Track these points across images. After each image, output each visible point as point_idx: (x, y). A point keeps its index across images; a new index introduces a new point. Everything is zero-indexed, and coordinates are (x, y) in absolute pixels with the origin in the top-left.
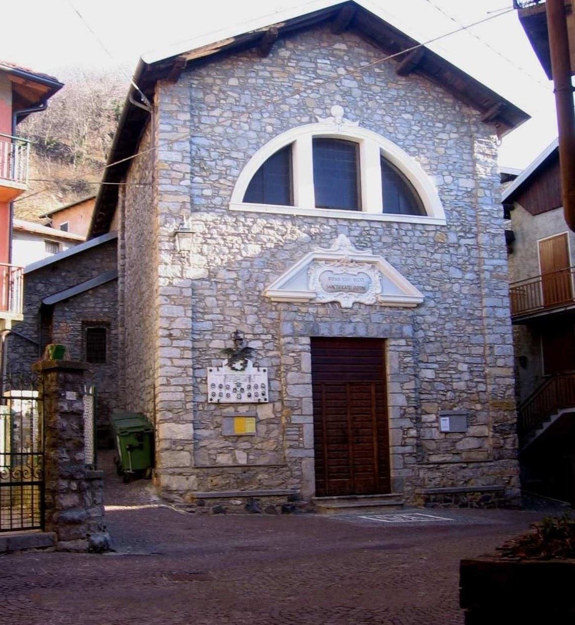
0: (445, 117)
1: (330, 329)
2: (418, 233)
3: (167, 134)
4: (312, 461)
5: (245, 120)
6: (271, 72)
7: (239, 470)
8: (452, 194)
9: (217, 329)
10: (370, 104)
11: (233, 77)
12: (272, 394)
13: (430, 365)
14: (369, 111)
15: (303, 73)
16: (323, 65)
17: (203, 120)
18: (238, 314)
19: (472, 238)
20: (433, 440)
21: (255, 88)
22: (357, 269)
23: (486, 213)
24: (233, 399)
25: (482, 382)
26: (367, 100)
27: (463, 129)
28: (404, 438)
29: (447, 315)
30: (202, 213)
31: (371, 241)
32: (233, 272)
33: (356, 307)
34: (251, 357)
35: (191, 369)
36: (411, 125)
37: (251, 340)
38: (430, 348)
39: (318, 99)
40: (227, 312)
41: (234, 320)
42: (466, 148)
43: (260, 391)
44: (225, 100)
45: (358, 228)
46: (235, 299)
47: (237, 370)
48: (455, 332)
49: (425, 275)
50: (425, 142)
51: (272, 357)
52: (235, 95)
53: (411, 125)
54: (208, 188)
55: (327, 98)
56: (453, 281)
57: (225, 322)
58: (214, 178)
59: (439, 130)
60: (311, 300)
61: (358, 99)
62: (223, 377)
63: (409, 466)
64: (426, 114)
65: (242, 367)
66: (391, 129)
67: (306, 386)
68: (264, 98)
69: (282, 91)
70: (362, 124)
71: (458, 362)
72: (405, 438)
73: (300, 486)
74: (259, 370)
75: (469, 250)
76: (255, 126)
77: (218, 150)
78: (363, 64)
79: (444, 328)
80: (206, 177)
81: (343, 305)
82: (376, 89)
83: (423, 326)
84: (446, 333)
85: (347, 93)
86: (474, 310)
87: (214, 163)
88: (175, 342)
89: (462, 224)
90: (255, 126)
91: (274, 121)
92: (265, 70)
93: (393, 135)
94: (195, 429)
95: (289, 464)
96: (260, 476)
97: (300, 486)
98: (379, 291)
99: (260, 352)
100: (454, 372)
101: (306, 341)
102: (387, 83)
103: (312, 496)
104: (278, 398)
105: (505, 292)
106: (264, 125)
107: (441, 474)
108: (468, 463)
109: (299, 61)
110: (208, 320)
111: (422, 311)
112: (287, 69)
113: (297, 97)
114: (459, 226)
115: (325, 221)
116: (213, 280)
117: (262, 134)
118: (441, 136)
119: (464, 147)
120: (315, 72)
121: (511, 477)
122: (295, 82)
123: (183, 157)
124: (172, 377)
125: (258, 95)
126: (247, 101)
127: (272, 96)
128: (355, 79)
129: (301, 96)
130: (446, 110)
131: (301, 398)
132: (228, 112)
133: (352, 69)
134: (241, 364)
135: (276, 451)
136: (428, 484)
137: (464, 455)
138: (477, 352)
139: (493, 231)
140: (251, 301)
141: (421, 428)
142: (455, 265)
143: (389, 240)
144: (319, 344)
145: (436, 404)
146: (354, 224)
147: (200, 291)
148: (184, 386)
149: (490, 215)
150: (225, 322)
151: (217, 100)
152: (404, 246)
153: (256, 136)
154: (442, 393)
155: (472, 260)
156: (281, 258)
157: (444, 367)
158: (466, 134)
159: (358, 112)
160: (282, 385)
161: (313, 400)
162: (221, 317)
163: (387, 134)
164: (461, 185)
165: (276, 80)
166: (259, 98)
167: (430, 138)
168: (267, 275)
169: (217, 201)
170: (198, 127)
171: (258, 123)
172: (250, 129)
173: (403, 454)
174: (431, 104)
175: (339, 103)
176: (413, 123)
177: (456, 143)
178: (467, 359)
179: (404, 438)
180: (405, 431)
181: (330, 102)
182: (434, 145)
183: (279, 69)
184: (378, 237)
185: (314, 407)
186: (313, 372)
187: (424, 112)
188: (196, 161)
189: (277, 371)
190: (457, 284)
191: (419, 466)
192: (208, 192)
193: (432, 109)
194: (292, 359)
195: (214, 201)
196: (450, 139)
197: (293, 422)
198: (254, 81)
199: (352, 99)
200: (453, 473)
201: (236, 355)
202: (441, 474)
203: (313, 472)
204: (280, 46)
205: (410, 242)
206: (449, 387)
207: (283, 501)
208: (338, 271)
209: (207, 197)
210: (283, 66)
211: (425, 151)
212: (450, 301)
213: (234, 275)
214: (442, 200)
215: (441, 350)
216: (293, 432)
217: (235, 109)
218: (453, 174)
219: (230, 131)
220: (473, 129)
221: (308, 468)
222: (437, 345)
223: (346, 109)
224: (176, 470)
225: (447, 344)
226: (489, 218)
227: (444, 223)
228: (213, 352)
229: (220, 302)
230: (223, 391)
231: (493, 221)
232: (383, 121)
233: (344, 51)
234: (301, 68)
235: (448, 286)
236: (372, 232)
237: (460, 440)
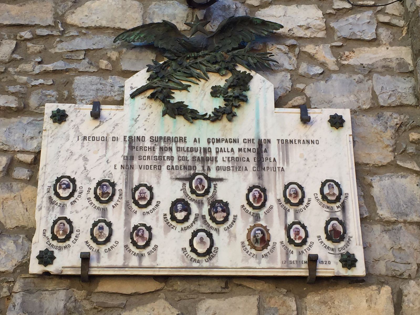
24: (170, 251)
34: (265, 66)
43: (315, 217)
47: (192, 116)
51: (369, 71)
62: (121, 149)
65: (219, 103)
74: (305, 120)
99: (310, 49)
134: (215, 92)
228: (82, 44)
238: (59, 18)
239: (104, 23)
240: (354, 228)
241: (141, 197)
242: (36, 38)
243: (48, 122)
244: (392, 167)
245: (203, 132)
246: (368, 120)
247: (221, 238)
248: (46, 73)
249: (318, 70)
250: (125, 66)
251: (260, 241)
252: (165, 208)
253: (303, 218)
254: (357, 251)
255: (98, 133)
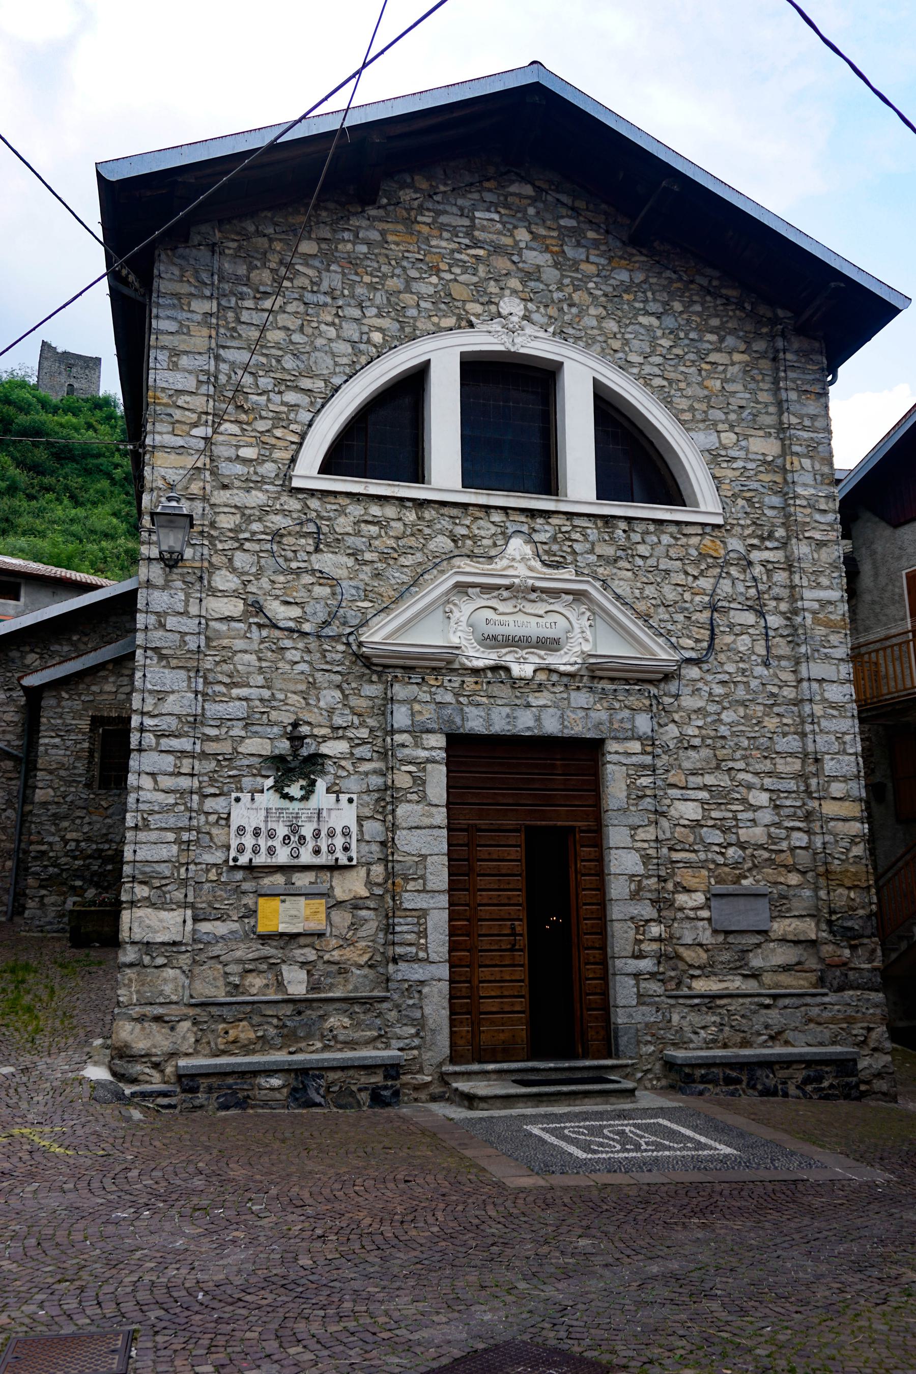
0: (722, 323)
1: (488, 720)
2: (666, 539)
3: (170, 337)
4: (445, 986)
5: (329, 319)
6: (383, 233)
7: (288, 1010)
8: (735, 466)
9: (258, 716)
10: (576, 297)
11: (310, 238)
12: (365, 848)
13: (692, 794)
14: (574, 310)
15: (446, 235)
16: (485, 223)
17: (245, 316)
18: (303, 687)
19: (776, 548)
20: (701, 945)
21: (354, 262)
22: (544, 604)
23: (805, 503)
24: (283, 857)
25: (799, 829)
26: (570, 289)
27: (760, 346)
28: (638, 942)
29: (727, 695)
30: (235, 491)
31: (574, 553)
32: (295, 607)
33: (542, 677)
34: (323, 773)
35: (195, 797)
36: (655, 338)
37: (325, 739)
38: (692, 759)
39: (475, 284)
40: (278, 684)
41: (294, 698)
42: (763, 380)
43: (339, 841)
44: (291, 280)
45: (547, 527)
46: (297, 659)
47: (292, 799)
48: (743, 728)
49: (680, 617)
50: (682, 369)
51: (366, 774)
52: (311, 272)
53: (655, 338)
54: (251, 445)
55: (492, 283)
56: (737, 629)
57: (275, 703)
58: (262, 426)
59: (710, 347)
60: (450, 662)
61: (553, 287)
62: (263, 813)
63: (647, 999)
64: (685, 316)
65: (303, 793)
66: (616, 345)
67: (436, 832)
68: (367, 279)
69: (404, 269)
70: (561, 334)
71: (750, 787)
72: (641, 941)
73: (417, 1042)
74: (338, 800)
75: (768, 571)
76: (351, 330)
77: (272, 375)
78: (562, 222)
79: (720, 720)
80: (247, 423)
81: (517, 670)
82: (591, 269)
83: (676, 717)
84: (723, 730)
85: (530, 275)
86: (780, 687)
87: (264, 398)
88: (163, 741)
89: (754, 523)
90: (351, 330)
91: (385, 323)
92: (371, 227)
93: (620, 355)
94: (196, 920)
95: (396, 996)
96: (332, 1021)
97: (417, 1042)
98: (587, 648)
99: (343, 763)
100: (741, 808)
101: (438, 741)
102: (610, 259)
103: (441, 1064)
104: (376, 856)
105: (841, 652)
106: (365, 329)
107: (716, 1019)
108: (775, 997)
109: (439, 213)
110: (240, 699)
111: (673, 687)
112: (417, 227)
113: (434, 280)
114: (748, 526)
115: (482, 515)
116: (251, 620)
117: (363, 347)
118: (713, 357)
119: (760, 377)
120: (468, 234)
121: (869, 1029)
122: (430, 252)
123: (200, 382)
124: (152, 812)
125: (357, 274)
126: (333, 284)
127: (385, 276)
128: (547, 250)
129: (441, 279)
130: (726, 310)
131: (424, 857)
132: (295, 303)
133: (542, 231)
135: (370, 966)
136: (692, 1041)
137: (767, 978)
138: (788, 769)
139: (818, 536)
140: (327, 663)
141: (674, 920)
142: (741, 599)
143: (609, 551)
144: (464, 749)
145: (705, 872)
146: (540, 521)
147: (225, 642)
148: (178, 830)
149: (809, 506)
150: (275, 703)
151: (274, 280)
152: (639, 562)
153: (350, 350)
154: (717, 849)
155: (776, 590)
156: (393, 581)
157: (719, 797)
158: (763, 355)
159: (552, 311)
160: (387, 829)
161: (449, 860)
162: (266, 694)
163: (607, 353)
164: (753, 448)
165: (393, 246)
166: (358, 279)
167: (693, 361)
168: (363, 611)
169: (268, 469)
170: (234, 329)
171: (355, 326)
172: (338, 337)
173: (636, 976)
174: (695, 298)
175: (514, 292)
176: (659, 333)
177: (746, 372)
178: (768, 782)
179: (638, 942)
180: (641, 925)
181: (497, 290)
182: (700, 375)
183: (400, 227)
184: (588, 546)
185: (450, 875)
186: (449, 805)
187: (681, 313)
188: (225, 393)
189: (378, 800)
190: (743, 637)
191: (672, 1001)
192: (249, 453)
193: (698, 308)
194: (408, 778)
195: (260, 470)
196: (733, 364)
197: (405, 905)
198: (349, 246)
199: (542, 286)
200: (743, 1016)
201: (291, 770)
202: (716, 1019)
203: (446, 1013)
204: (403, 186)
205: (651, 555)
206: (733, 839)
207: (377, 1079)
208: (502, 607)
209: (245, 461)
210: (410, 222)
211: (682, 385)
212: (730, 668)
213: (296, 612)
214: (714, 477)
215: (714, 764)
216: (404, 927)
217: (309, 297)
218: (737, 430)
219: (296, 338)
220: (780, 344)
221: (436, 1007)
222: (705, 752)
223: (530, 305)
224: (148, 1010)
225: (725, 751)
226: (808, 511)
227: (719, 521)
228: (246, 762)
229: (264, 664)
230: (262, 842)
231: (818, 517)
232: (600, 328)
233: (528, 197)
234: (442, 227)
235: (729, 639)
236: (575, 536)
237: (758, 945)
238: (235, 749)
239: (254, 752)
240: (354, 845)
241: (271, 835)
242: (225, 759)
243: (233, 802)
244: (372, 817)
245: (296, 805)
246: (365, 797)
247: (302, 850)
248: (230, 776)
249: (345, 774)
250: (264, 773)
251: (317, 852)
252: (281, 838)
253: (335, 842)
254: (354, 855)
255: (254, 806)
